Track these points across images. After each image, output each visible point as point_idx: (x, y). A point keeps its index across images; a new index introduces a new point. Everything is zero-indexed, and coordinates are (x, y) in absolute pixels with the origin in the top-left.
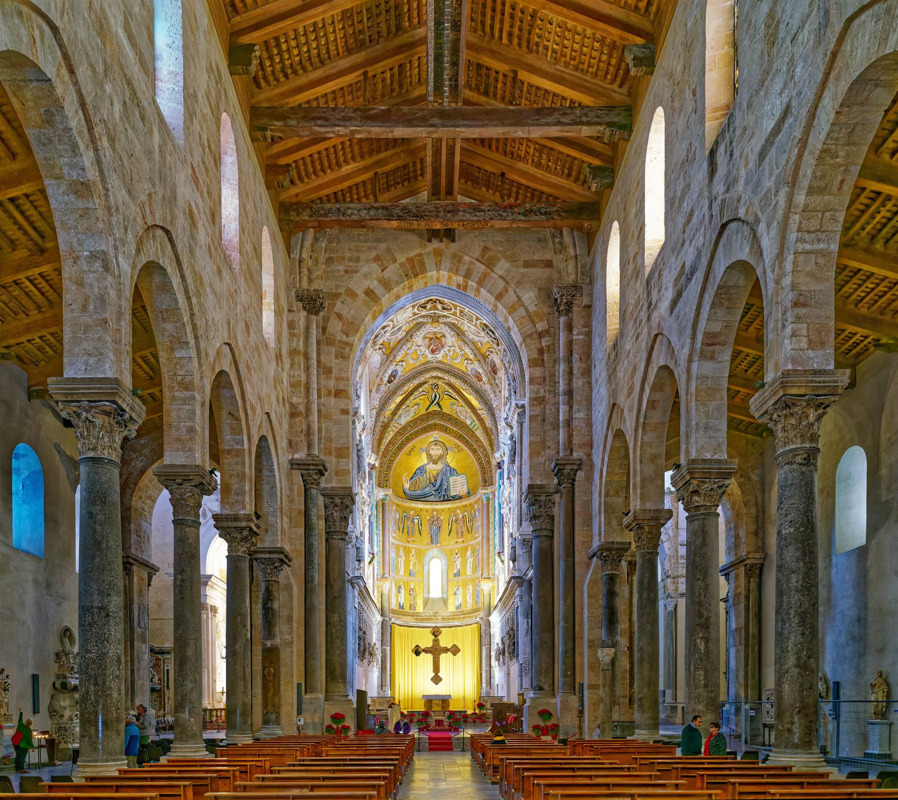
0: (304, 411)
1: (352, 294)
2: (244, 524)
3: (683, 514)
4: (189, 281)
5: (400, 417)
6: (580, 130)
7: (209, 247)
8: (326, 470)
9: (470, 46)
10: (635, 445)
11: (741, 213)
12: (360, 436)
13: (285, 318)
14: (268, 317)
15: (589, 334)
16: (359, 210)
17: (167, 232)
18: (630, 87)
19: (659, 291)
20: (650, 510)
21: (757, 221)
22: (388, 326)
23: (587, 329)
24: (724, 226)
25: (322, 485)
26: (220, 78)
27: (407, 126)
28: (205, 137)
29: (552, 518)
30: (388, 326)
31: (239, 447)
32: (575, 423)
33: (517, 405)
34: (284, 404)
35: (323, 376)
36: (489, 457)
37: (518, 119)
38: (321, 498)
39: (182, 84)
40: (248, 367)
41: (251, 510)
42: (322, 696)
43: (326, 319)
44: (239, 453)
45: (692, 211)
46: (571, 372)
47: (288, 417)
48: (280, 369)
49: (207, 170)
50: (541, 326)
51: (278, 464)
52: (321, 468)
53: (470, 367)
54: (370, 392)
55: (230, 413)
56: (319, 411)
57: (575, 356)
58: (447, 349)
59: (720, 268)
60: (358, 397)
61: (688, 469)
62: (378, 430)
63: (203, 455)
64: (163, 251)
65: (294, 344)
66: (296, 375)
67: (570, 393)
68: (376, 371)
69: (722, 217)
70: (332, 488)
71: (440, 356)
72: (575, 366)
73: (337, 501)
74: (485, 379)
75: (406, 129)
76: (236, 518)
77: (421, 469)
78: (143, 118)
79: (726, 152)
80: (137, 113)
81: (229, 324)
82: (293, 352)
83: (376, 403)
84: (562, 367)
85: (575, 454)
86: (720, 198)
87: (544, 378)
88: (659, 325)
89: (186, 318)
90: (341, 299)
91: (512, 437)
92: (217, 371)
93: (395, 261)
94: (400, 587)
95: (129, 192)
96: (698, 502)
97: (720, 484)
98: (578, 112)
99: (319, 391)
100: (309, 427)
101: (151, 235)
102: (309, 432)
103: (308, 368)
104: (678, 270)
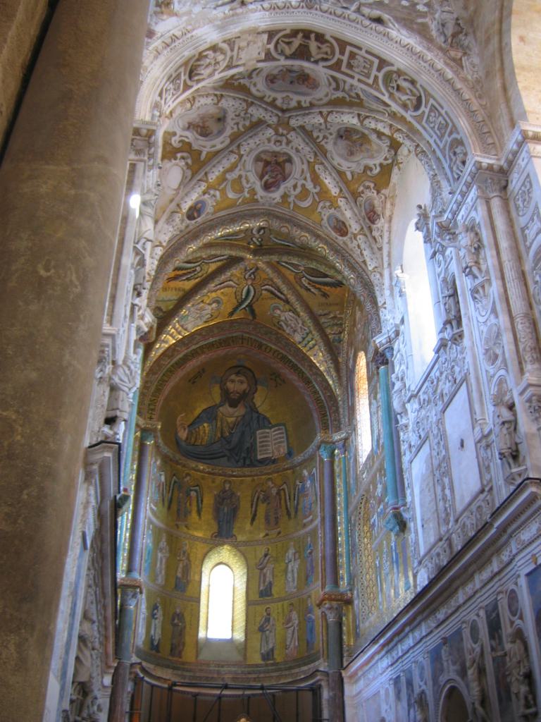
53: (326, 214)
68: (170, 193)
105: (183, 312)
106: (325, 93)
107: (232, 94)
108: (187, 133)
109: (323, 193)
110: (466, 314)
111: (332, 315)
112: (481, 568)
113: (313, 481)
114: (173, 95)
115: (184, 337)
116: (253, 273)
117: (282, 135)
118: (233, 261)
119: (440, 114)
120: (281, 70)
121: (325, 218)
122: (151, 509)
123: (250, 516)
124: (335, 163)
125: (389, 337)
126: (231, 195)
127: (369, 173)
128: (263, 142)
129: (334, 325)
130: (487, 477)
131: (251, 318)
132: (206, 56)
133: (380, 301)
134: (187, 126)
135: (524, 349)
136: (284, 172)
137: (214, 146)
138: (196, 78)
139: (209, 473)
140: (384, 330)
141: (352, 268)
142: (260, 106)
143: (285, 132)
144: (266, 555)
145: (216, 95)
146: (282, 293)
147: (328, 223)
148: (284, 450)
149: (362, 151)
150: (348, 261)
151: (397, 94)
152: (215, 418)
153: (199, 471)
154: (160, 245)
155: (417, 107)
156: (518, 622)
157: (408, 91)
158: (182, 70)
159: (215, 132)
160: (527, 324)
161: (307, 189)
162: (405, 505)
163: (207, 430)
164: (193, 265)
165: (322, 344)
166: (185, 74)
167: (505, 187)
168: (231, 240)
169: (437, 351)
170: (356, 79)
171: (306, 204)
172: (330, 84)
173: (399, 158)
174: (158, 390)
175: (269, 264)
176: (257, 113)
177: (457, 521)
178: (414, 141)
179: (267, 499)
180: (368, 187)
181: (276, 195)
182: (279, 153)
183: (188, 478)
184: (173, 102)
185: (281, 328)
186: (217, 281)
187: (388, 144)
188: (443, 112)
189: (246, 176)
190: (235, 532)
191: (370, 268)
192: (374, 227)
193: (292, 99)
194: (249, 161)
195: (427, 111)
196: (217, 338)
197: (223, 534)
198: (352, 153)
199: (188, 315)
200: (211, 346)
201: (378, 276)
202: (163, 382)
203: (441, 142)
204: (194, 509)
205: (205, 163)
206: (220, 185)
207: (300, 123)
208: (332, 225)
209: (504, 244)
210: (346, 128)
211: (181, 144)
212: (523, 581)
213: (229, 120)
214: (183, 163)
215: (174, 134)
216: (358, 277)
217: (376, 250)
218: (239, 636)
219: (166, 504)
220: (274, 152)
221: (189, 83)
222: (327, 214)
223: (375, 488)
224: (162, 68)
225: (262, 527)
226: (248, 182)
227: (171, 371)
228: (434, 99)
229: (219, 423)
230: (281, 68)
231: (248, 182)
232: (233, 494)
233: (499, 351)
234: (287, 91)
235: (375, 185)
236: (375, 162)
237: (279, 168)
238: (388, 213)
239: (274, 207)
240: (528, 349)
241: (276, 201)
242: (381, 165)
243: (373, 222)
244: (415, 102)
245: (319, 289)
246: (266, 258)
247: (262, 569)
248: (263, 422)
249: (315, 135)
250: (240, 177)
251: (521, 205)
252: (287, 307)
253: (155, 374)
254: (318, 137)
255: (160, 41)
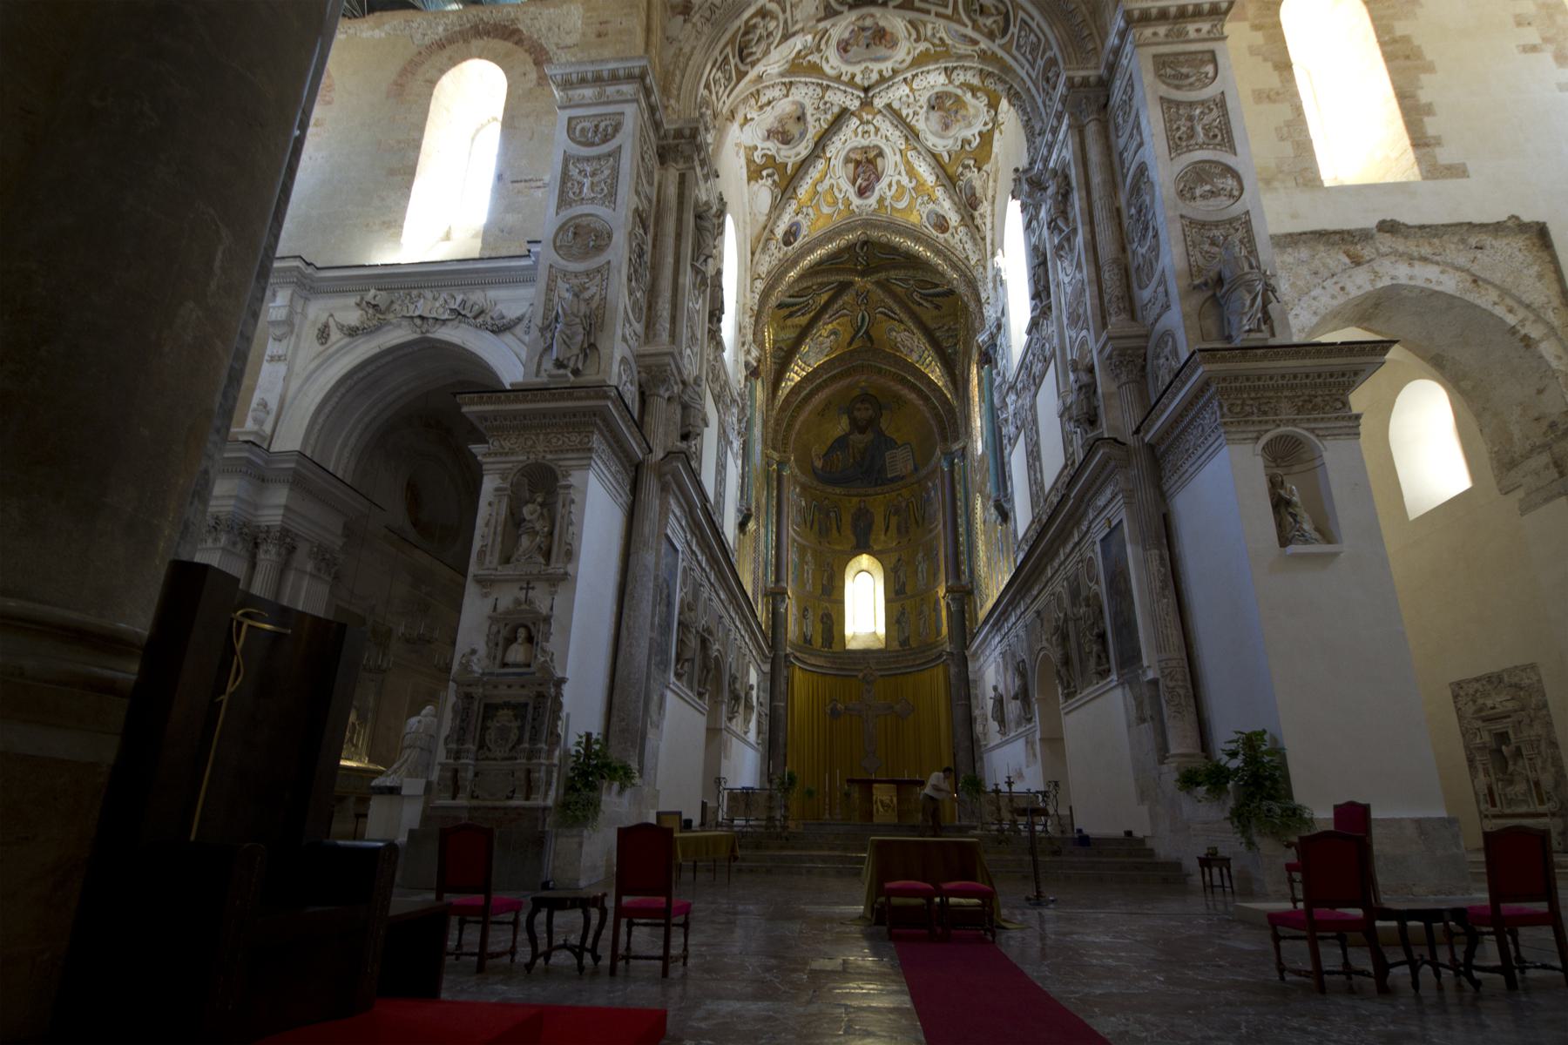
54: (753, 254)
68: (763, 219)
94: (806, 610)
105: (804, 349)
106: (906, 50)
107: (803, 79)
108: (769, 144)
109: (919, 187)
110: (1054, 280)
111: (946, 327)
112: (1064, 543)
113: (936, 492)
114: (726, 87)
115: (808, 374)
116: (865, 297)
117: (868, 122)
118: (843, 287)
119: (1031, 30)
120: (853, 31)
121: (924, 216)
122: (794, 530)
123: (884, 528)
124: (929, 144)
125: (991, 333)
126: (826, 210)
127: (967, 147)
128: (848, 139)
129: (948, 337)
130: (1071, 450)
131: (869, 345)
132: (755, 26)
133: (983, 296)
134: (766, 134)
135: (1110, 301)
136: (877, 170)
137: (799, 154)
138: (749, 60)
139: (845, 495)
140: (987, 327)
141: (955, 267)
142: (839, 89)
143: (870, 117)
144: (899, 560)
145: (784, 84)
146: (895, 314)
147: (928, 219)
148: (910, 467)
149: (958, 121)
150: (950, 260)
151: (981, 20)
153: (836, 494)
154: (759, 277)
155: (1005, 31)
156: (1096, 587)
157: (993, 11)
158: (729, 49)
159: (797, 136)
160: (1116, 271)
161: (903, 186)
162: (1006, 496)
163: (841, 457)
164: (805, 299)
165: (937, 359)
166: (734, 57)
167: (1106, 106)
168: (837, 263)
169: (1029, 332)
170: (933, 14)
171: (902, 205)
172: (910, 35)
173: (999, 118)
174: (790, 426)
175: (878, 283)
176: (838, 98)
177: (1045, 501)
178: (1005, 82)
179: (897, 512)
180: (967, 167)
181: (872, 201)
182: (869, 147)
183: (827, 502)
184: (728, 97)
185: (898, 350)
186: (830, 312)
187: (986, 102)
188: (1034, 25)
189: (838, 184)
190: (871, 543)
191: (973, 263)
192: (976, 214)
193: (872, 71)
194: (837, 163)
195: (1016, 31)
196: (839, 370)
197: (862, 547)
198: (946, 127)
199: (808, 351)
200: (833, 379)
201: (981, 269)
202: (793, 418)
203: (1034, 69)
204: (835, 526)
205: (793, 177)
206: (811, 200)
207: (885, 101)
208: (932, 223)
209: (1097, 179)
210: (937, 93)
211: (764, 159)
212: (1098, 548)
213: (809, 118)
214: (770, 181)
215: (756, 148)
216: (960, 276)
217: (979, 240)
219: (808, 525)
220: (862, 148)
221: (742, 68)
222: (926, 211)
223: (986, 486)
224: (703, 52)
226: (840, 191)
227: (800, 407)
228: (1024, 10)
229: (851, 451)
230: (851, 27)
231: (840, 191)
232: (868, 511)
233: (1081, 311)
234: (865, 60)
235: (976, 161)
236: (972, 132)
237: (871, 167)
238: (990, 193)
239: (872, 215)
240: (1114, 299)
241: (872, 208)
242: (980, 134)
243: (975, 209)
244: (1002, 24)
245: (931, 302)
246: (875, 277)
247: (896, 572)
248: (891, 444)
249: (904, 113)
250: (832, 186)
251: (1121, 122)
252: (902, 327)
254: (908, 115)
255: (698, 16)
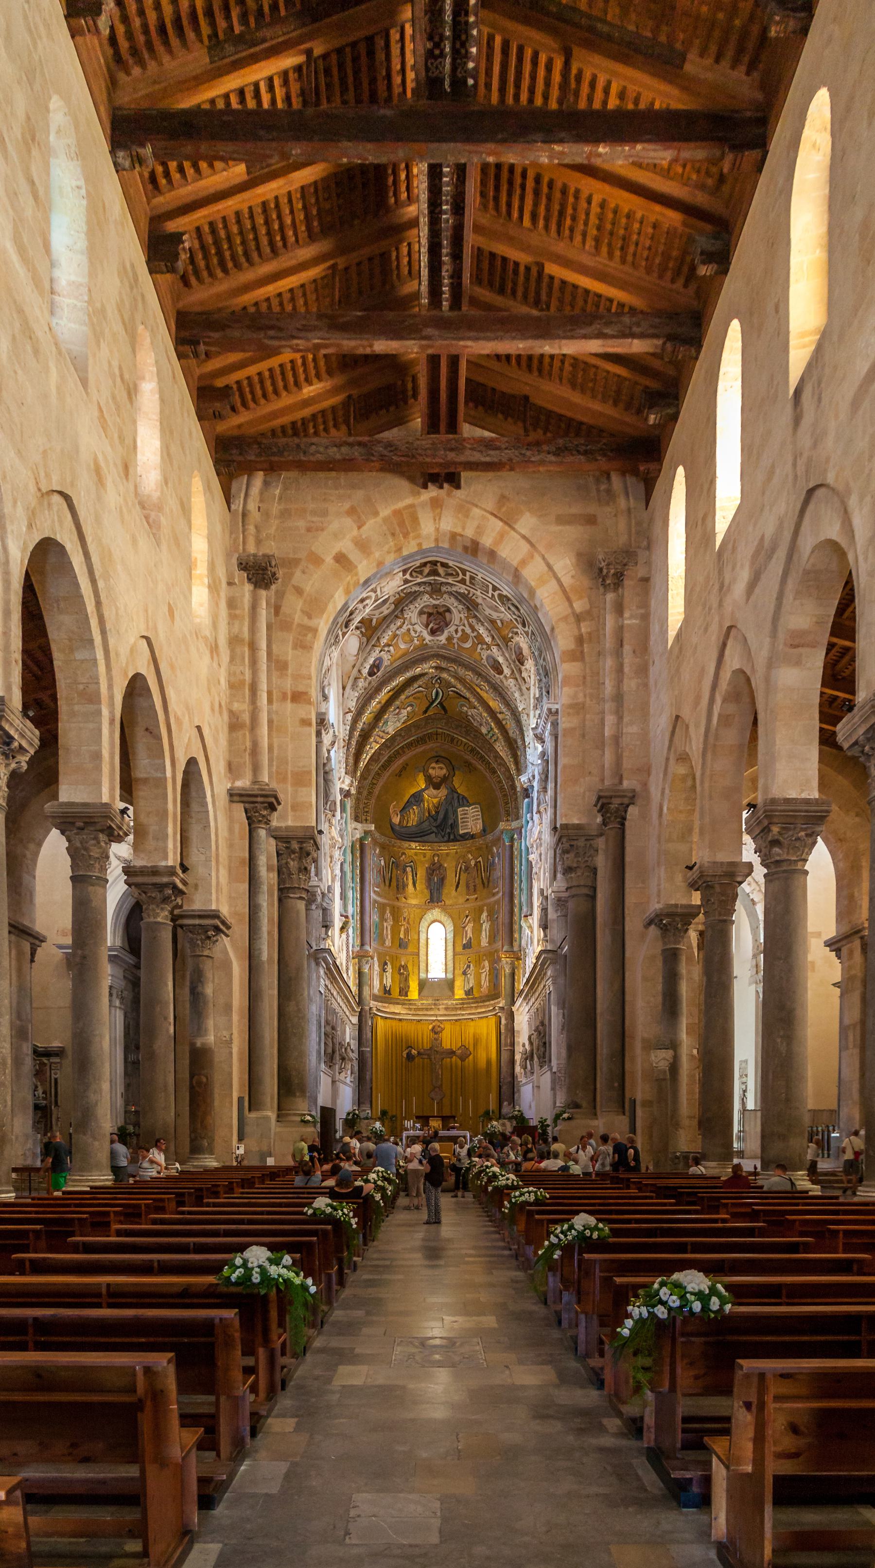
0: (248, 722)
1: (317, 560)
2: (165, 880)
3: (760, 871)
4: (95, 559)
5: (386, 722)
6: (631, 344)
7: (121, 508)
8: (279, 803)
9: (478, 229)
10: (703, 774)
11: (830, 479)
12: (329, 751)
13: (223, 594)
14: (200, 595)
15: (645, 617)
16: (326, 447)
17: (67, 498)
18: (698, 288)
19: (733, 569)
20: (722, 863)
21: (849, 492)
22: (367, 598)
23: (642, 611)
24: (811, 492)
25: (274, 823)
26: (136, 280)
27: (392, 339)
28: (115, 364)
29: (594, 871)
30: (367, 598)
31: (159, 775)
32: (625, 740)
33: (550, 710)
34: (221, 713)
35: (275, 674)
36: (513, 780)
37: (543, 330)
38: (273, 842)
39: (86, 298)
40: (172, 667)
41: (175, 860)
42: (272, 1114)
43: (280, 595)
44: (161, 783)
45: (773, 466)
46: (620, 670)
47: (226, 729)
48: (215, 665)
49: (118, 408)
50: (579, 606)
51: (213, 796)
52: (273, 800)
54: (344, 688)
55: (147, 729)
56: (270, 722)
57: (627, 648)
58: (452, 629)
59: (807, 542)
60: (325, 698)
61: (765, 811)
62: (354, 743)
63: (112, 789)
64: (61, 522)
65: (236, 629)
66: (238, 672)
67: (618, 698)
69: (807, 481)
70: (287, 828)
71: (442, 638)
72: (626, 661)
73: (295, 846)
74: (507, 671)
75: (389, 342)
76: (154, 871)
77: (417, 798)
78: (36, 352)
79: (813, 394)
80: (29, 348)
81: (146, 611)
82: (234, 641)
83: (352, 704)
84: (609, 663)
85: (626, 784)
86: (805, 455)
87: (584, 678)
88: (733, 613)
89: (90, 607)
90: (300, 567)
91: (543, 754)
92: (130, 675)
93: (376, 514)
94: (386, 964)
95: (19, 452)
96: (779, 855)
97: (809, 832)
98: (626, 320)
99: (270, 694)
100: (255, 746)
101: (46, 503)
102: (255, 751)
103: (254, 662)
104: (756, 543)
152: (422, 801)
185: (469, 721)
197: (435, 897)
200: (410, 745)
201: (525, 717)
218: (450, 976)
225: (465, 892)
248: (464, 801)
253: (365, 779)
